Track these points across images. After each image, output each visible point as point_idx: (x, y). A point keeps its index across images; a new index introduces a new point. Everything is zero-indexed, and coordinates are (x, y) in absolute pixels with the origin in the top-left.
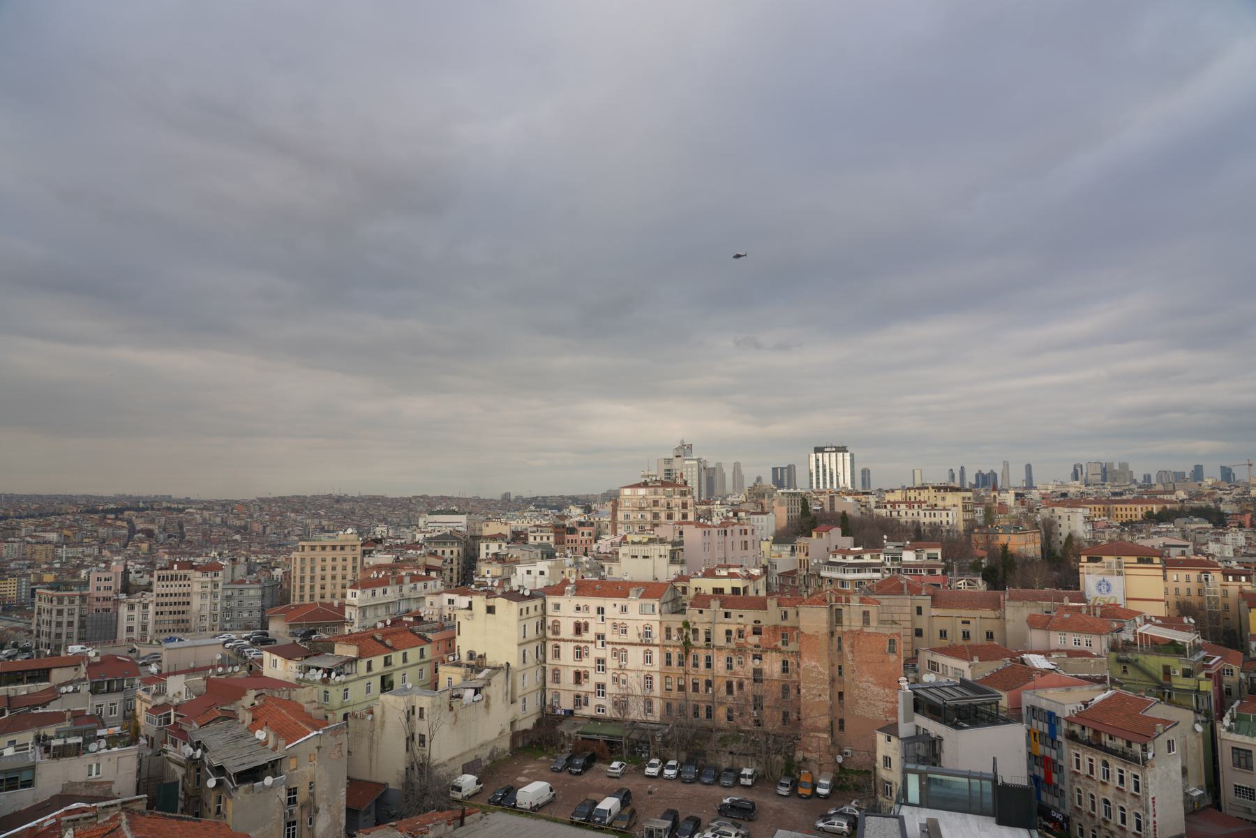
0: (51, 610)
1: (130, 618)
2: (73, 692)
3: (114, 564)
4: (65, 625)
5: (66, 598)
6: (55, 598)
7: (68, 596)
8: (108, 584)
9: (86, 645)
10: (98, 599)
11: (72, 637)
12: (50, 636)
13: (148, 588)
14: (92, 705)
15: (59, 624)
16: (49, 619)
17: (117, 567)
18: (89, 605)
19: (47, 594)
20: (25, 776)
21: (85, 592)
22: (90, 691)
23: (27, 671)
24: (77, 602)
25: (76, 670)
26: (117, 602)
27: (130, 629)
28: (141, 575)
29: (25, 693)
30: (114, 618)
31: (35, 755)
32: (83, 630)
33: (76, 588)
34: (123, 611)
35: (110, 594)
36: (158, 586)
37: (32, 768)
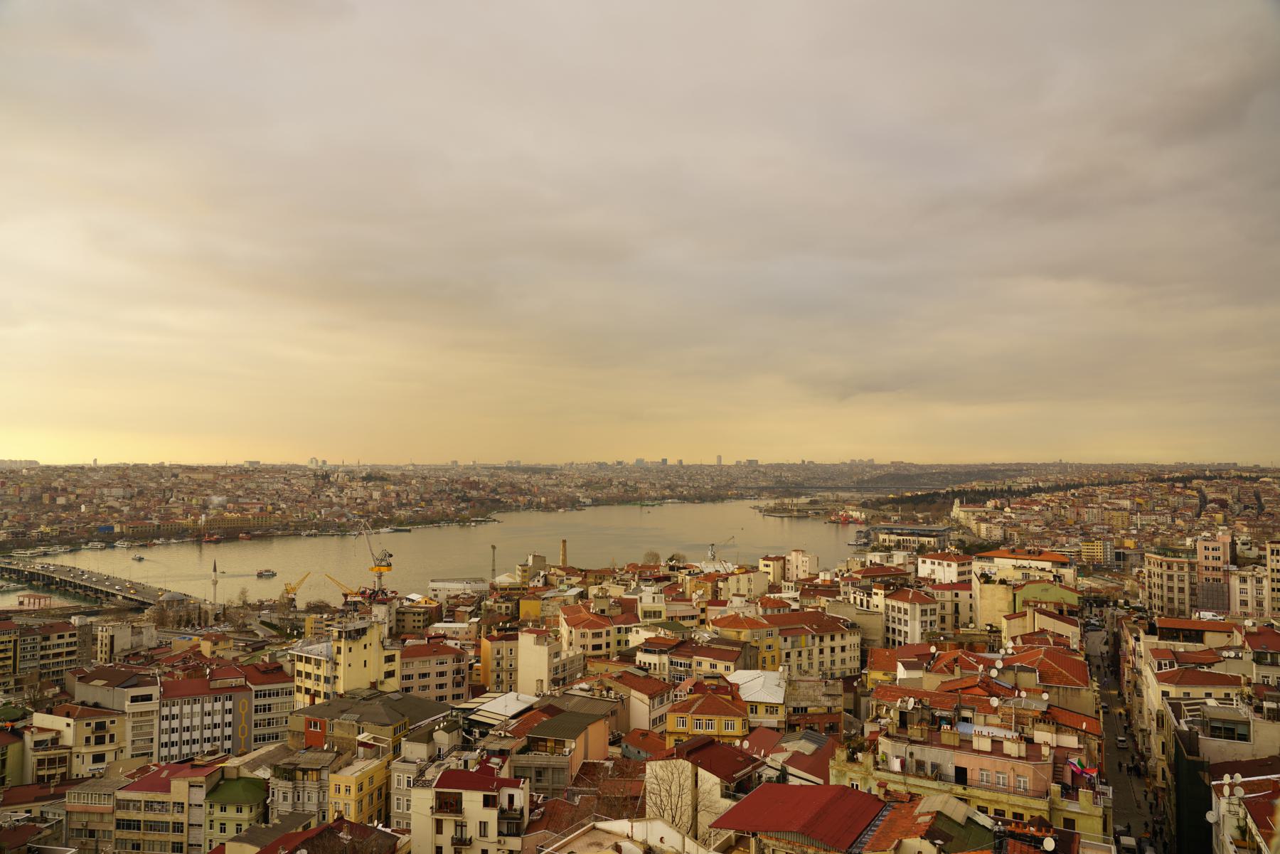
0: (1162, 574)
1: (1242, 591)
2: (1235, 658)
3: (1220, 533)
4: (1176, 591)
5: (1175, 564)
6: (1164, 564)
7: (1177, 562)
8: (1216, 554)
9: (1216, 612)
10: (1207, 568)
11: (1184, 603)
12: (1162, 600)
13: (1260, 561)
14: (1257, 674)
15: (1170, 589)
16: (1160, 583)
17: (1223, 536)
18: (1198, 573)
19: (1156, 559)
20: (1240, 730)
21: (1193, 560)
22: (1253, 660)
23: (1182, 630)
24: (1186, 569)
25: (1229, 636)
26: (1227, 573)
27: (1244, 603)
28: (1249, 547)
29: (1182, 650)
30: (1226, 590)
31: (1245, 711)
32: (1194, 597)
33: (1183, 556)
34: (1235, 582)
35: (1219, 564)
36: (1272, 561)
37: (1247, 723)
